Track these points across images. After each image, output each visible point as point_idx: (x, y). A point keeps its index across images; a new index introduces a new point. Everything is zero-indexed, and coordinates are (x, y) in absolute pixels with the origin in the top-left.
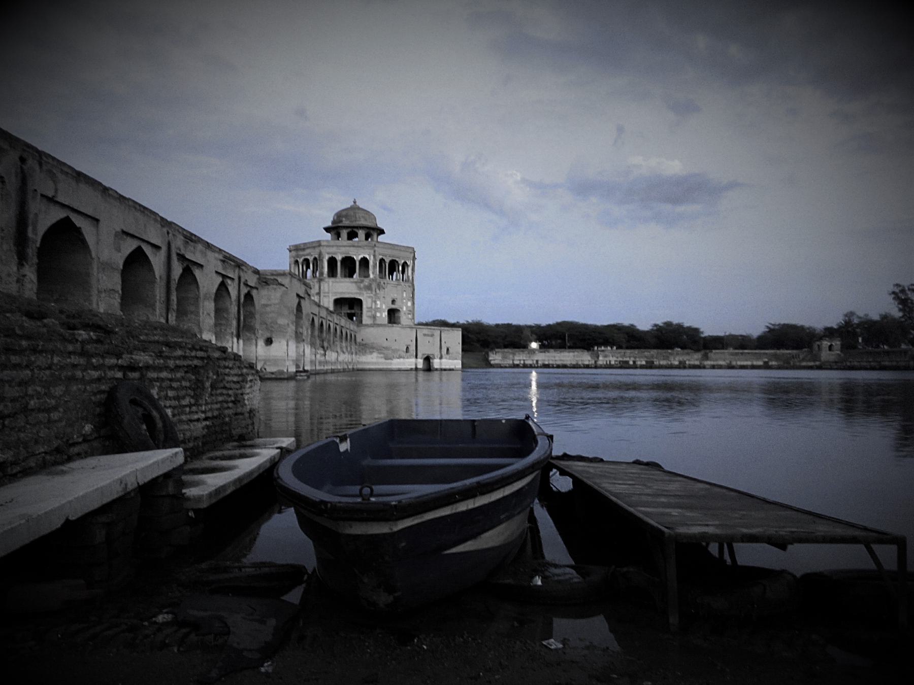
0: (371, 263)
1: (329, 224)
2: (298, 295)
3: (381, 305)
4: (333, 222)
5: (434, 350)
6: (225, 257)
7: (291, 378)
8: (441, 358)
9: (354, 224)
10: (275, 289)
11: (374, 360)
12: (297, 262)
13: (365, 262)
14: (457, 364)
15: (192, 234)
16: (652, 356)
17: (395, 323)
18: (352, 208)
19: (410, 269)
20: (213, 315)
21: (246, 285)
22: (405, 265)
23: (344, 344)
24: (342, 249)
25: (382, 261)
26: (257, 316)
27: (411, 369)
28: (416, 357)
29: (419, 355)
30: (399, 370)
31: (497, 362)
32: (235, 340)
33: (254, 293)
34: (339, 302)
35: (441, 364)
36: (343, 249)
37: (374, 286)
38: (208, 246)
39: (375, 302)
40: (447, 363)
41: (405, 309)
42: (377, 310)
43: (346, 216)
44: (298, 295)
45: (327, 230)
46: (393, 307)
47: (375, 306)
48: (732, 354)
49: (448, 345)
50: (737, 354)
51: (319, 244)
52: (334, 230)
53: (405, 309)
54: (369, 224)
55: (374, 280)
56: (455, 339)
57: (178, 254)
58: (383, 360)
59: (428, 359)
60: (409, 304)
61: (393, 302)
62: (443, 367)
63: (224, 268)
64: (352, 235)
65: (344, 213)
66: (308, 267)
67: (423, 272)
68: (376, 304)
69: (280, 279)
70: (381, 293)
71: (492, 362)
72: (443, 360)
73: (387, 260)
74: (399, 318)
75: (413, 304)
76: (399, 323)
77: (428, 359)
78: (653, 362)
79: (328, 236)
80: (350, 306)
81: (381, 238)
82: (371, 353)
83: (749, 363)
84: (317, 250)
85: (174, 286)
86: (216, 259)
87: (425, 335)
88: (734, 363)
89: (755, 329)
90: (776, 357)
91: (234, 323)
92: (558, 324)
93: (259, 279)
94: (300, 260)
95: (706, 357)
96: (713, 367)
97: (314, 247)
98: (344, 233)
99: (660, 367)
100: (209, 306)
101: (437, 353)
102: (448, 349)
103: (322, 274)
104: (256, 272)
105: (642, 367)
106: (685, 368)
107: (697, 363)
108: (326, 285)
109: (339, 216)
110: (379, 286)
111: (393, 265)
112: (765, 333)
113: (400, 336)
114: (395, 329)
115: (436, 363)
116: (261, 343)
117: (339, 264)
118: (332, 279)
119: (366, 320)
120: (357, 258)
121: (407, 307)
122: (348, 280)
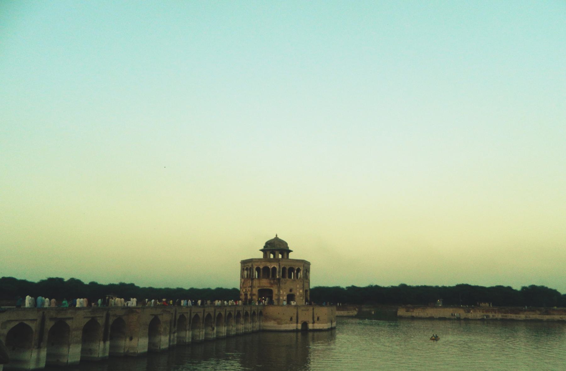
1: (262, 248)
3: (283, 292)
4: (264, 247)
8: (314, 323)
13: (274, 269)
22: (298, 270)
28: (297, 323)
29: (299, 321)
32: (102, 343)
35: (313, 326)
40: (318, 326)
54: (282, 247)
58: (276, 325)
59: (305, 324)
62: (315, 328)
69: (137, 310)
77: (305, 324)
111: (291, 270)
115: (310, 326)
116: (128, 339)
117: (261, 270)
121: (299, 293)
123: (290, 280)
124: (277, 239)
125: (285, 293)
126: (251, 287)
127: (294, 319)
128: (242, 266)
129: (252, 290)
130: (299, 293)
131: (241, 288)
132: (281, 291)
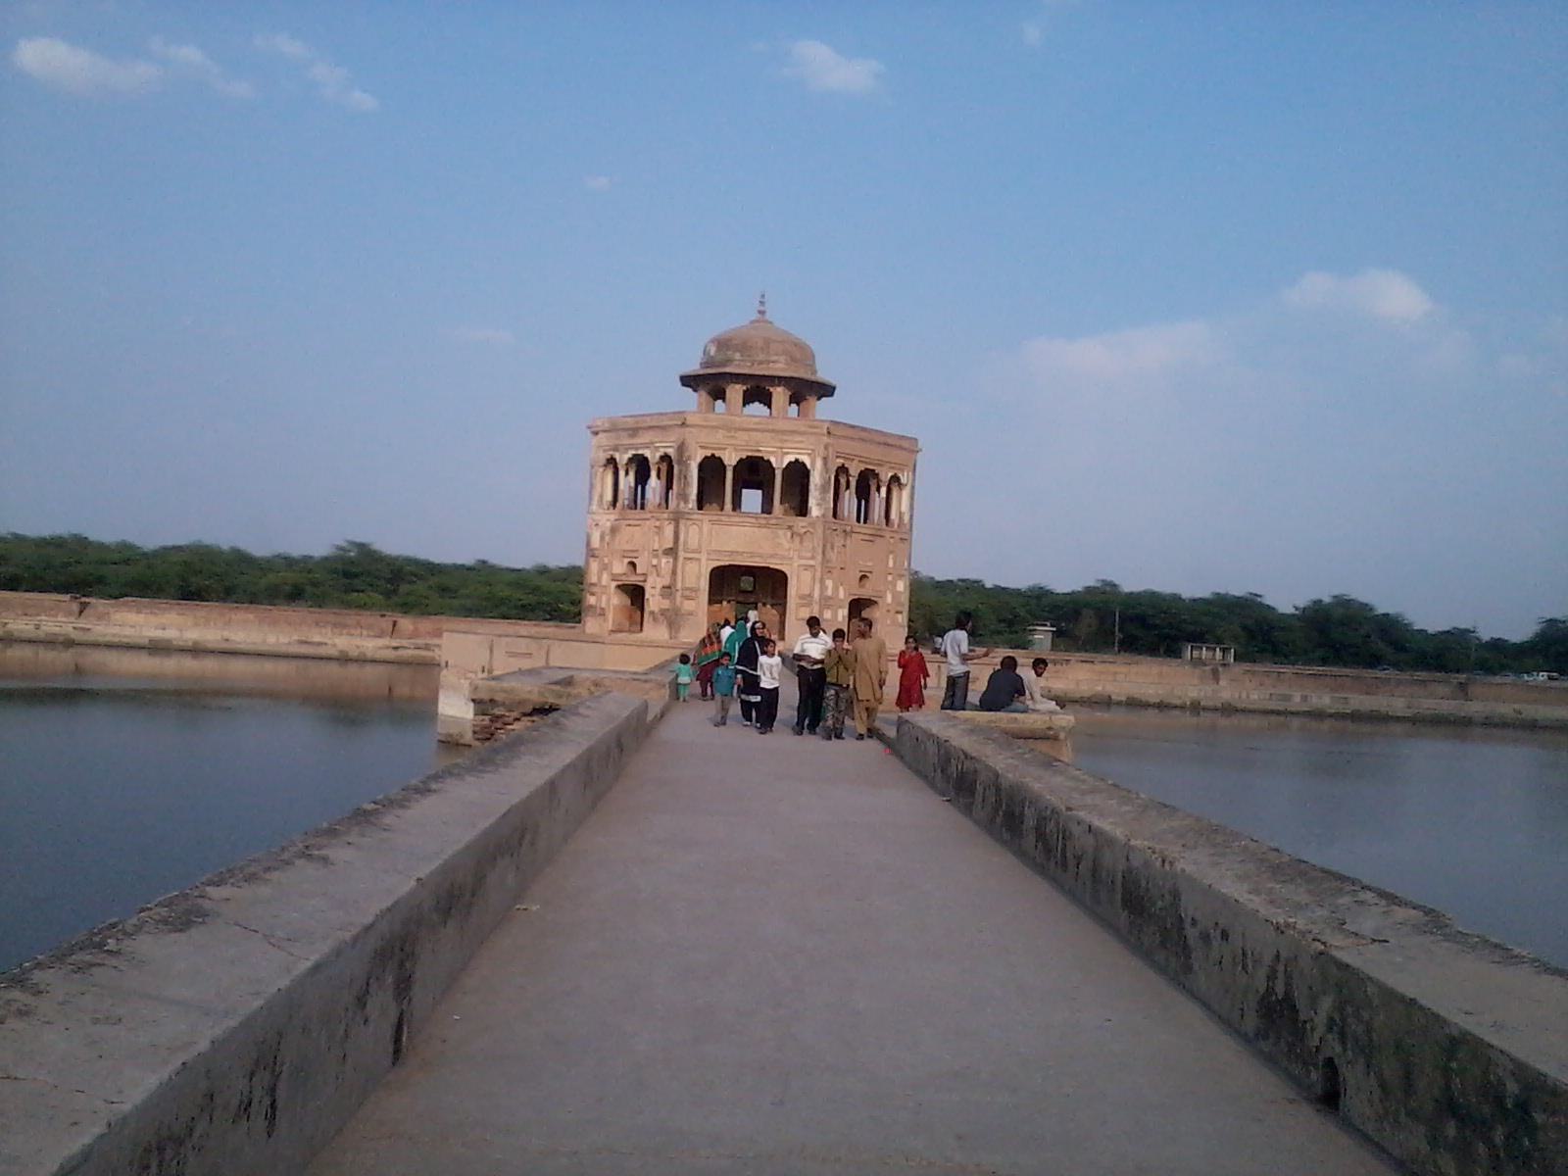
0: (816, 479)
1: (694, 367)
3: (836, 589)
13: (798, 475)
19: (906, 493)
24: (738, 431)
25: (842, 470)
36: (743, 436)
39: (822, 582)
41: (889, 599)
43: (744, 347)
45: (689, 381)
46: (865, 592)
52: (710, 383)
53: (889, 599)
73: (855, 471)
79: (691, 400)
94: (622, 458)
98: (735, 392)
108: (694, 530)
117: (729, 475)
120: (779, 462)
121: (895, 595)
123: (862, 528)
125: (841, 595)
126: (672, 552)
129: (674, 573)
131: (591, 553)
132: (829, 583)
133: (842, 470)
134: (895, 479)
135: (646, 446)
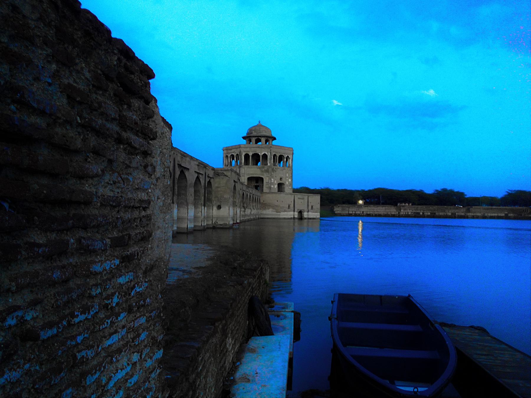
0: (269, 157)
1: (245, 135)
2: (234, 181)
4: (247, 134)
5: (303, 207)
6: (199, 163)
7: (231, 228)
8: (308, 212)
9: (259, 135)
10: (223, 178)
11: (270, 213)
12: (227, 156)
13: (265, 156)
14: (317, 215)
15: (185, 153)
16: (435, 210)
17: (281, 191)
18: (258, 126)
19: (290, 160)
20: (193, 195)
21: (209, 177)
23: (254, 204)
24: (252, 149)
25: (275, 156)
26: (213, 193)
27: (291, 218)
28: (294, 211)
30: (285, 219)
31: (338, 212)
33: (212, 180)
34: (250, 179)
35: (308, 215)
37: (270, 170)
38: (192, 158)
42: (272, 184)
43: (255, 131)
44: (234, 181)
45: (244, 138)
47: (271, 182)
48: (485, 209)
49: (312, 204)
50: (488, 209)
51: (239, 146)
52: (248, 138)
55: (270, 167)
56: (316, 200)
57: (178, 164)
59: (300, 212)
60: (290, 180)
61: (281, 179)
62: (310, 217)
63: (199, 169)
64: (258, 141)
65: (253, 128)
66: (233, 159)
67: (298, 161)
68: (271, 180)
69: (225, 173)
70: (274, 174)
71: (336, 212)
72: (310, 213)
73: (278, 155)
74: (284, 188)
75: (292, 180)
76: (284, 191)
77: (300, 212)
78: (435, 213)
79: (244, 142)
80: (257, 182)
81: (274, 143)
82: (269, 209)
83: (496, 215)
84: (238, 150)
85: (176, 181)
86: (195, 164)
87: (299, 198)
88: (486, 215)
89: (500, 194)
90: (513, 211)
91: (203, 198)
92: (376, 189)
93: (214, 173)
94: (229, 155)
95: (468, 211)
96: (473, 217)
97: (237, 148)
98: (253, 140)
99: (440, 217)
100: (191, 190)
101: (306, 209)
102: (312, 207)
103: (241, 163)
104: (213, 169)
105: (428, 217)
106: (455, 217)
107: (463, 214)
109: (251, 130)
110: (273, 170)
111: (281, 158)
112: (505, 195)
113: (286, 198)
114: (282, 195)
115: (305, 215)
116: (215, 208)
117: (251, 158)
118: (247, 166)
119: (265, 189)
120: (261, 154)
121: (289, 182)
122: (255, 166)
124: (260, 126)
127: (292, 206)
128: (224, 154)
130: (289, 182)
133: (275, 156)
134: (288, 156)
135: (233, 152)
